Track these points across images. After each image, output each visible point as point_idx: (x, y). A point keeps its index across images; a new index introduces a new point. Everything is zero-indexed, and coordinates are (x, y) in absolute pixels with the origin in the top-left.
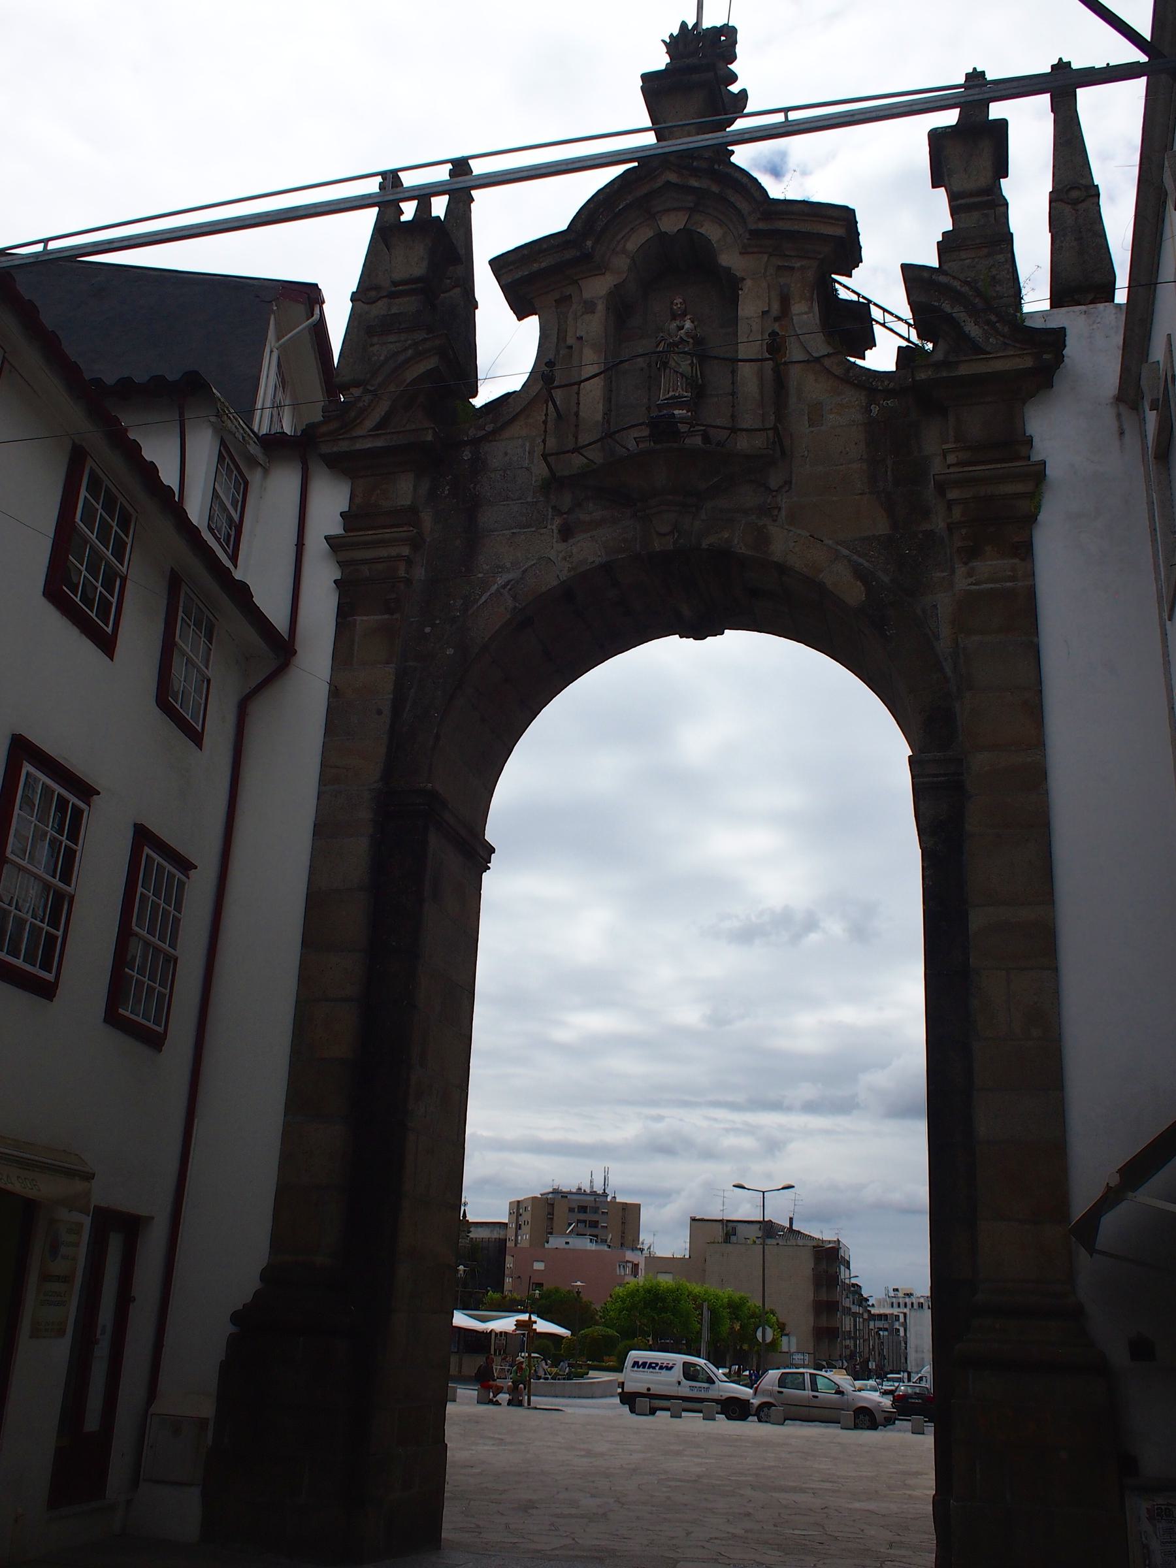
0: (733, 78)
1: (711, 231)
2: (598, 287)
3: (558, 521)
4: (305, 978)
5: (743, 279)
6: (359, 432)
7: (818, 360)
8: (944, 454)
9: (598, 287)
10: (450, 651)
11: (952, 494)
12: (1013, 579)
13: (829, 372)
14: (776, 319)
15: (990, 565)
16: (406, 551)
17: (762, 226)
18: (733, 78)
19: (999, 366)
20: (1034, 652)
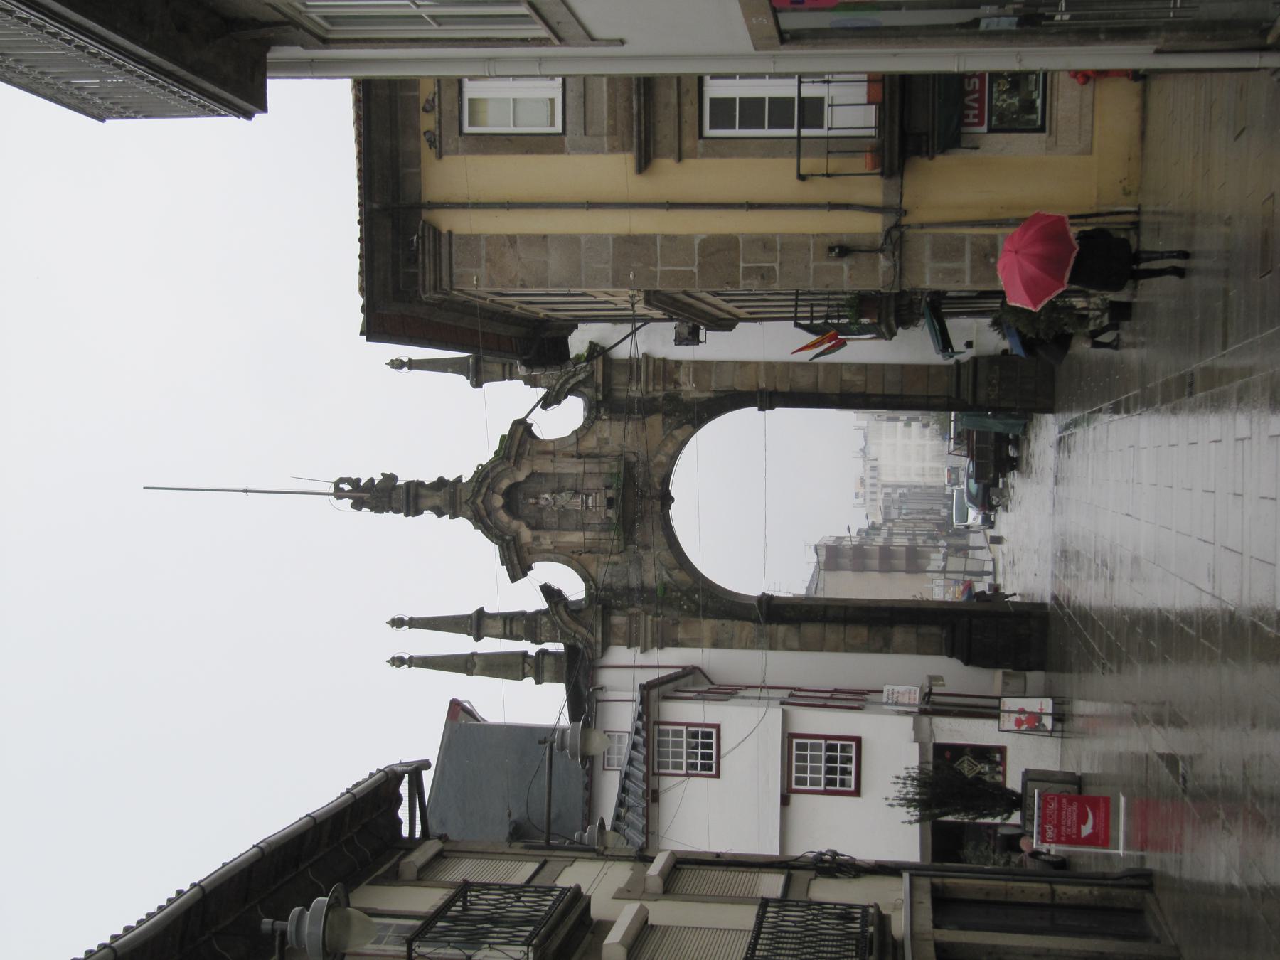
0: (372, 480)
1: (505, 484)
2: (526, 535)
3: (640, 551)
4: (836, 649)
5: (533, 471)
6: (593, 640)
7: (578, 439)
8: (631, 390)
9: (526, 535)
10: (697, 596)
11: (651, 389)
12: (689, 369)
13: (583, 436)
14: (555, 456)
15: (682, 376)
16: (650, 617)
17: (512, 461)
18: (372, 480)
19: (600, 367)
20: (720, 363)
